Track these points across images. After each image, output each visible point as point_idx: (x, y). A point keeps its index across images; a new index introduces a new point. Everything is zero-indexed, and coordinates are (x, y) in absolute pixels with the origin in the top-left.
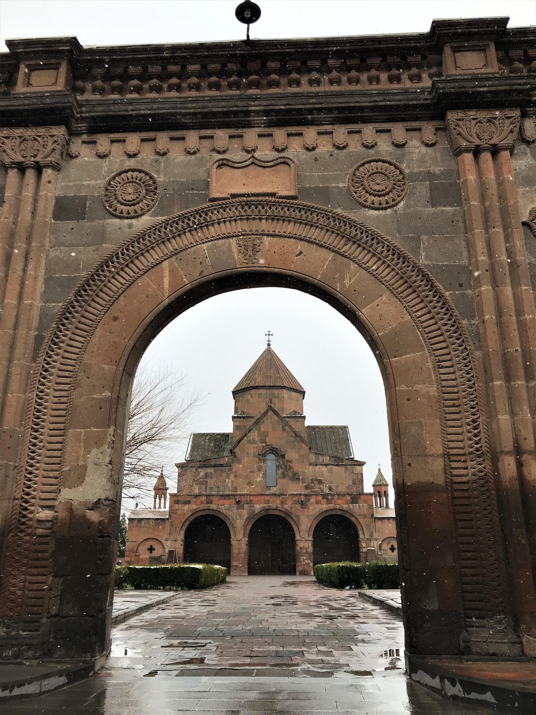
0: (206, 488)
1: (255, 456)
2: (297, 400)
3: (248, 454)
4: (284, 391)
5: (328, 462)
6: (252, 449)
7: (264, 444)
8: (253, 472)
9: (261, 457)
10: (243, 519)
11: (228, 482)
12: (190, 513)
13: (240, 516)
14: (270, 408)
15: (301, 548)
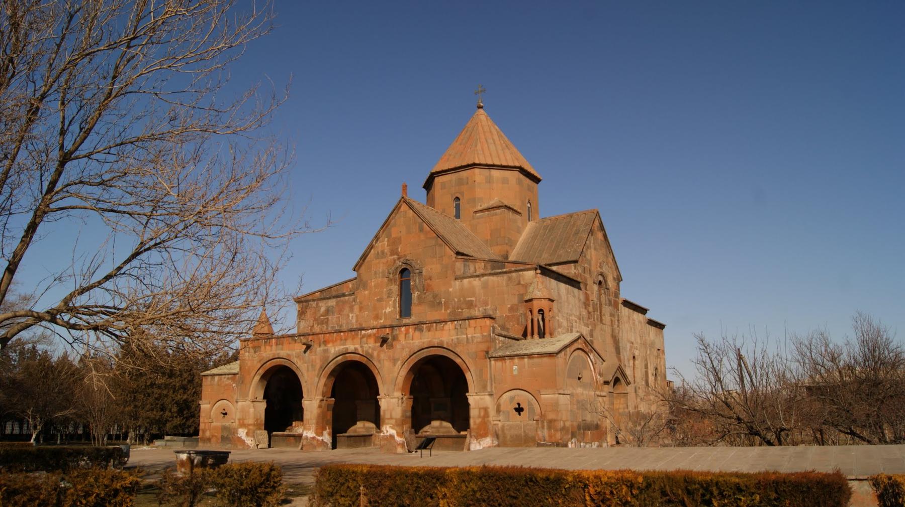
0: (327, 329)
1: (383, 276)
2: (505, 181)
3: (376, 273)
4: (477, 171)
5: (482, 271)
6: (382, 268)
7: (396, 257)
8: (380, 300)
9: (391, 276)
10: (314, 370)
11: (353, 316)
12: (259, 365)
13: (312, 365)
14: (404, 200)
15: (384, 411)
